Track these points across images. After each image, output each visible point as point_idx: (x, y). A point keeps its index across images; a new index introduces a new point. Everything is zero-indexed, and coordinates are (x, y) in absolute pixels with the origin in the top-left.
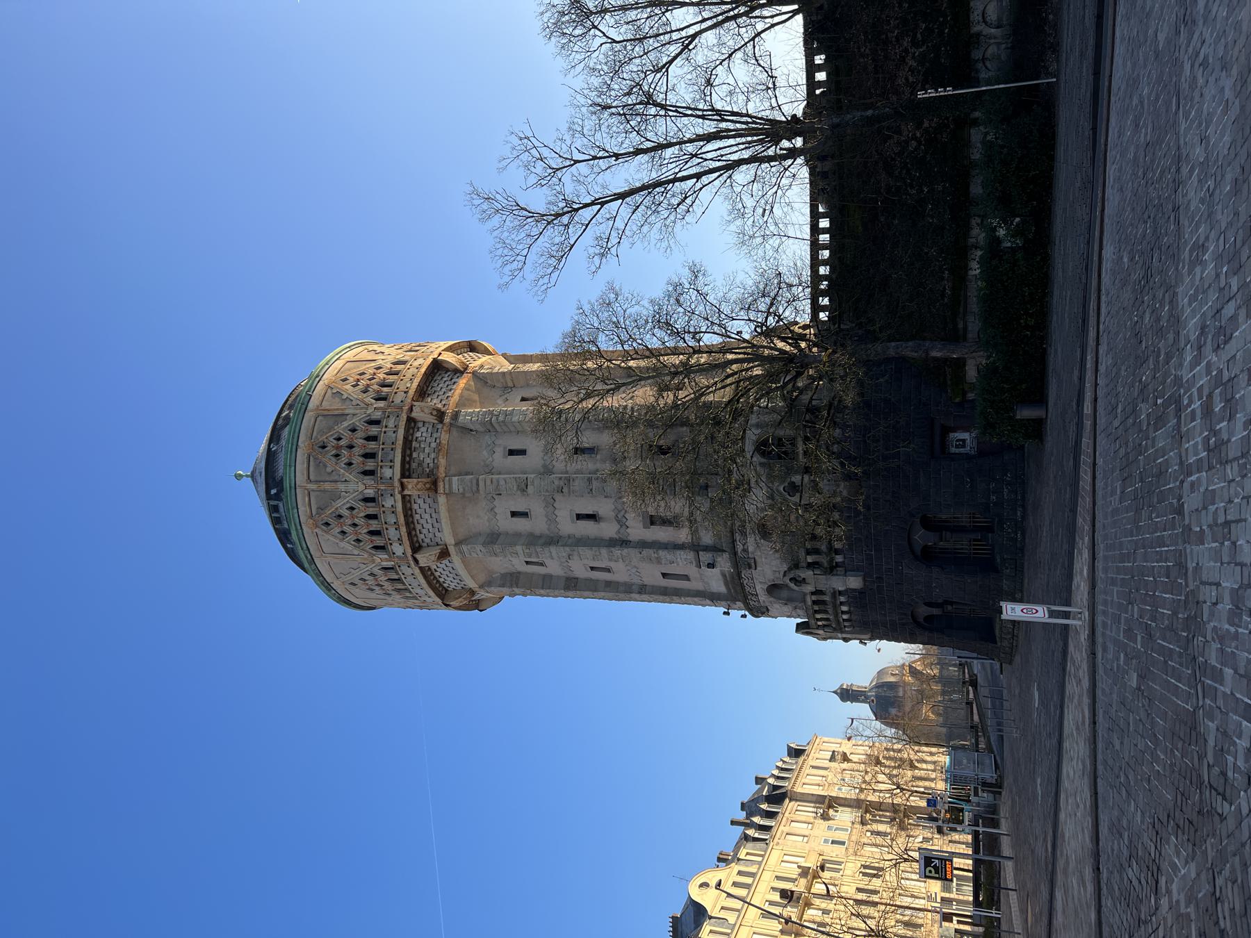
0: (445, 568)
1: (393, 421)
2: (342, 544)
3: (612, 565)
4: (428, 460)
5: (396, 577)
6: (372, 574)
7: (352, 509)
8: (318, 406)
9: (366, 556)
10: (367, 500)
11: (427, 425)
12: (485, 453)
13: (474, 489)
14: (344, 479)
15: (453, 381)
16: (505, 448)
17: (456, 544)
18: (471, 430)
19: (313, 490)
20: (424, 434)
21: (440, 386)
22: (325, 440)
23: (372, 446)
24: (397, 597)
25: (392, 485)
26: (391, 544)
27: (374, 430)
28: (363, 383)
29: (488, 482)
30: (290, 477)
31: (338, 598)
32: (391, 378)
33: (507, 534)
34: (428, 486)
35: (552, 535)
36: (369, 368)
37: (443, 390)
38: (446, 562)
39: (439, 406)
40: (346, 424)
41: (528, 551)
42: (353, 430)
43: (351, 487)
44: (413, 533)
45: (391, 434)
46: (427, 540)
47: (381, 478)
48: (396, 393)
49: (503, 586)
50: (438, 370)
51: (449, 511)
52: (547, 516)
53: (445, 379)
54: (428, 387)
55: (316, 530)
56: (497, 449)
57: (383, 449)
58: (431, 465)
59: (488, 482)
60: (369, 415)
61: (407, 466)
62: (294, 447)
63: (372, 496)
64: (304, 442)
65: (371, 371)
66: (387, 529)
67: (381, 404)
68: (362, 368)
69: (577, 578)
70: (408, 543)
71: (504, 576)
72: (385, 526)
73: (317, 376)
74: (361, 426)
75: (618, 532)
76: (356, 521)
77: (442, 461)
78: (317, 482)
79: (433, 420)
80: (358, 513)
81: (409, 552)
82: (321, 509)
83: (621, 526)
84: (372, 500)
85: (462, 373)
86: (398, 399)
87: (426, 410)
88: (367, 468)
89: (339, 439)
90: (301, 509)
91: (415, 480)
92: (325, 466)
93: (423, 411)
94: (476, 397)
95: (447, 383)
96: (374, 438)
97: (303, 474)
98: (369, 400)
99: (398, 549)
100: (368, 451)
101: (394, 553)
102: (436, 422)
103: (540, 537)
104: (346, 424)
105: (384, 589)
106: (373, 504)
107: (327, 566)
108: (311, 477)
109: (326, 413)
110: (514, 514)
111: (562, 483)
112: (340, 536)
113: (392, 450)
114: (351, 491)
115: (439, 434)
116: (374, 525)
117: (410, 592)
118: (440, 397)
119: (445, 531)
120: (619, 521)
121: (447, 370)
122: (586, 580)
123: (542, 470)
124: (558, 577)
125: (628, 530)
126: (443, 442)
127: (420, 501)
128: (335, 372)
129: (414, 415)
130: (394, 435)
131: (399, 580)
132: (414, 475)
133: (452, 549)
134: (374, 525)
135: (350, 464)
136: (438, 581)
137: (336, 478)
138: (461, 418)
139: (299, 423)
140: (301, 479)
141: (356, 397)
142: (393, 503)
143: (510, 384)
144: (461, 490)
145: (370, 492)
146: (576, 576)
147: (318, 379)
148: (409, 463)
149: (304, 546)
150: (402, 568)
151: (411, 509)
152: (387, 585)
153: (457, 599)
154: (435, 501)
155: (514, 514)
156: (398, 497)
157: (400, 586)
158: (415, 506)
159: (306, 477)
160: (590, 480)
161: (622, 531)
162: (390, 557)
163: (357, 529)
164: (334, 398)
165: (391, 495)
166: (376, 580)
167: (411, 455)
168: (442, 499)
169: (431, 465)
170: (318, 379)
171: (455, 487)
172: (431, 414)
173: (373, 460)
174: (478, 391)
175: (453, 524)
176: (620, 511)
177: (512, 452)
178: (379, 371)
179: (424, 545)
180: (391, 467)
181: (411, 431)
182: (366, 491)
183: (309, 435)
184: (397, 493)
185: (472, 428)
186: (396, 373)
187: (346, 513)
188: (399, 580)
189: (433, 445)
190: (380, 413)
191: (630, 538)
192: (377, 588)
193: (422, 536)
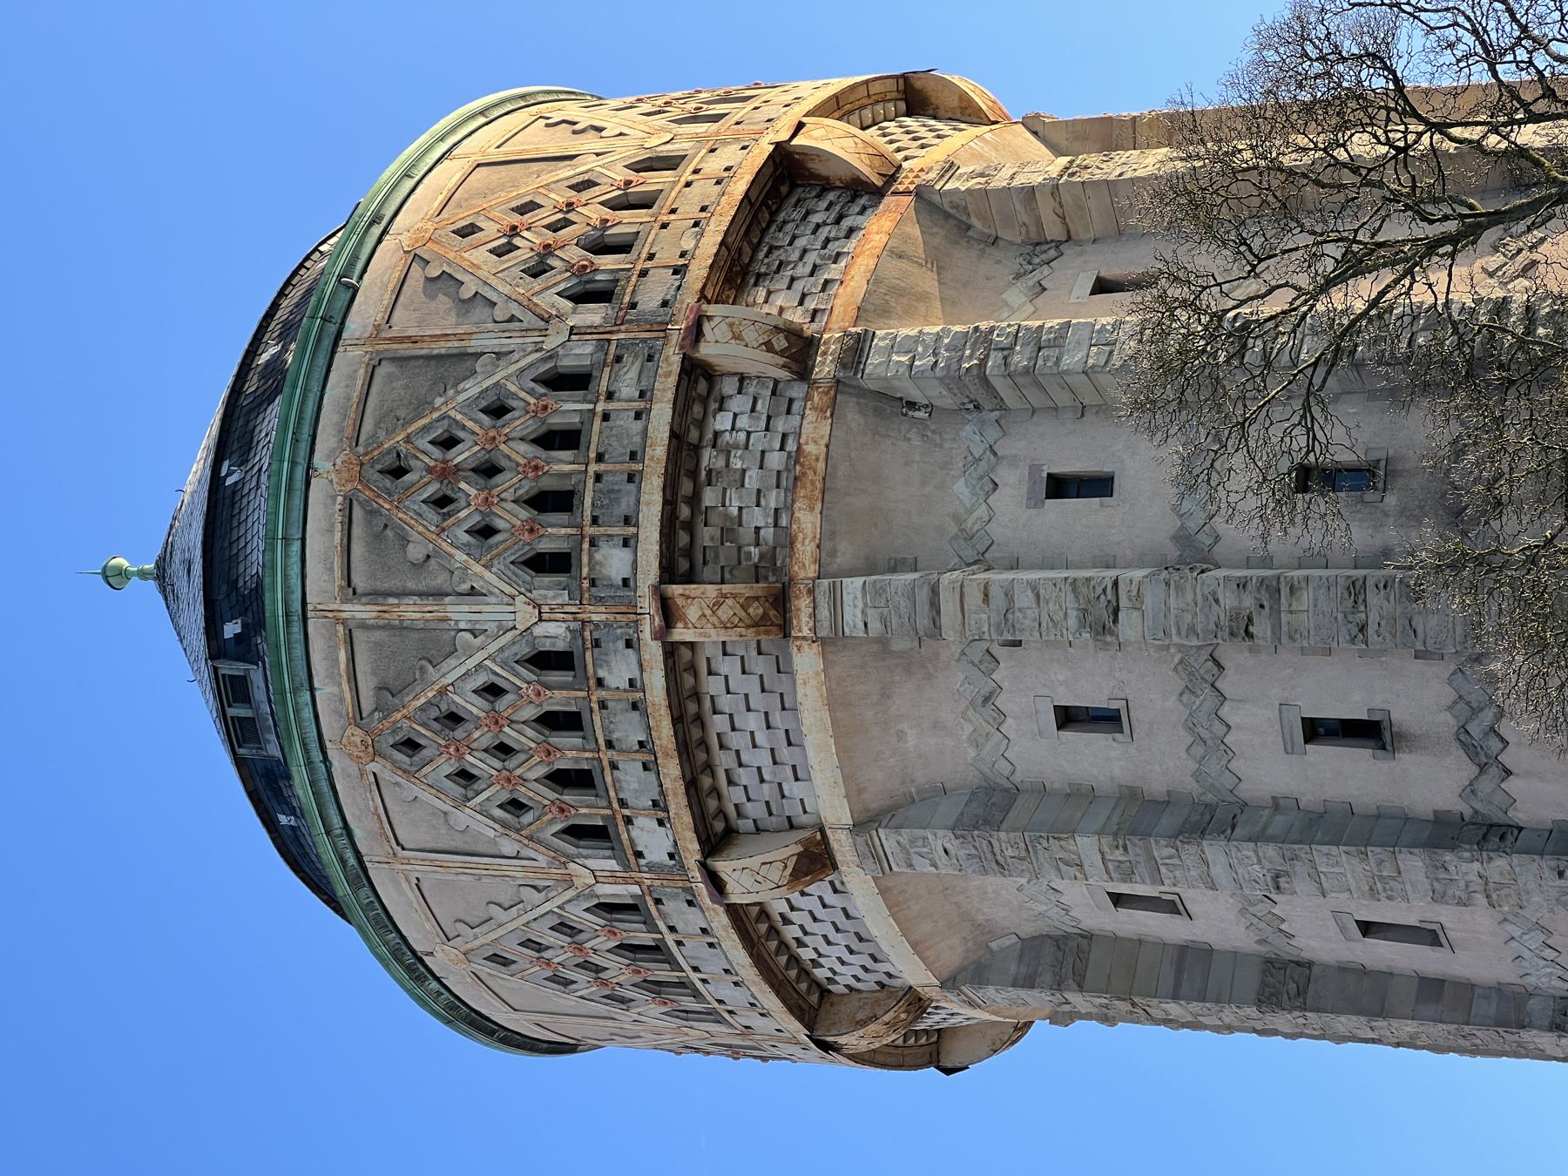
0: (820, 912)
1: (633, 374)
2: (463, 817)
3: (1444, 916)
4: (757, 518)
5: (646, 938)
6: (563, 927)
7: (493, 691)
8: (377, 327)
9: (542, 861)
10: (544, 660)
11: (751, 389)
12: (961, 488)
13: (923, 622)
14: (465, 587)
15: (846, 223)
16: (1034, 469)
17: (862, 825)
18: (912, 405)
19: (363, 626)
20: (743, 422)
21: (801, 243)
22: (403, 448)
23: (562, 463)
24: (651, 1011)
25: (632, 608)
27: (568, 409)
28: (530, 241)
29: (974, 597)
30: (286, 577)
31: (451, 1007)
32: (628, 222)
33: (1042, 791)
34: (756, 610)
35: (1209, 798)
36: (551, 187)
37: (811, 258)
38: (820, 888)
39: (797, 317)
40: (471, 388)
41: (1118, 855)
43: (491, 613)
45: (625, 422)
46: (755, 810)
47: (593, 583)
48: (644, 273)
49: (1029, 982)
50: (793, 187)
51: (835, 702)
52: (1191, 727)
53: (816, 218)
54: (755, 249)
55: (373, 767)
56: (1005, 475)
57: (598, 478)
58: (768, 534)
59: (974, 597)
60: (552, 355)
61: (683, 539)
62: (300, 472)
63: (561, 646)
64: (331, 455)
65: (561, 197)
66: (614, 766)
67: (593, 315)
68: (527, 184)
69: (1310, 965)
70: (687, 818)
71: (1032, 946)
72: (606, 754)
73: (374, 221)
74: (522, 393)
75: (1470, 790)
76: (510, 735)
77: (807, 521)
78: (376, 595)
79: (770, 367)
82: (389, 691)
83: (1483, 768)
85: (878, 193)
86: (650, 297)
87: (750, 335)
88: (545, 546)
89: (449, 443)
90: (325, 691)
91: (711, 591)
92: (404, 540)
93: (737, 337)
94: (927, 281)
95: (824, 232)
96: (566, 439)
98: (551, 301)
99: (652, 841)
100: (548, 484)
101: (639, 855)
102: (783, 374)
103: (1167, 803)
104: (471, 388)
105: (605, 983)
107: (413, 896)
108: (356, 579)
109: (404, 349)
110: (1067, 717)
111: (1248, 602)
112: (456, 790)
113: (631, 478)
114: (492, 627)
115: (795, 420)
116: (570, 751)
117: (697, 995)
118: (799, 286)
119: (817, 776)
120: (1471, 750)
121: (825, 185)
122: (1343, 969)
123: (1173, 553)
124: (1235, 954)
125: (1511, 785)
126: (809, 448)
127: (729, 666)
128: (437, 204)
129: (706, 351)
130: (639, 425)
131: (656, 951)
132: (707, 573)
133: (842, 844)
134: (570, 751)
135: (485, 532)
136: (794, 960)
137: (441, 580)
138: (874, 360)
139: (316, 388)
140: (321, 583)
141: (506, 290)
142: (636, 674)
143: (1053, 230)
144: (875, 627)
146: (1306, 955)
147: (376, 231)
148: (689, 527)
149: (336, 822)
150: (668, 906)
151: (696, 695)
152: (618, 970)
153: (863, 1024)
154: (782, 667)
155: (1067, 717)
156: (653, 651)
157: (662, 973)
158: (713, 686)
159: (339, 580)
160: (1356, 590)
161: (1486, 785)
162: (626, 867)
163: (511, 764)
164: (432, 297)
166: (579, 947)
167: (694, 500)
168: (806, 661)
169: (768, 534)
170: (376, 231)
171: (852, 617)
172: (769, 347)
173: (563, 517)
174: (937, 262)
175: (844, 753)
176: (1475, 711)
177: (1059, 487)
178: (585, 195)
179: (745, 825)
180: (626, 543)
181: (697, 410)
183: (349, 432)
184: (646, 634)
185: (915, 395)
186: (646, 202)
187: (474, 706)
188: (656, 951)
189: (776, 460)
190: (589, 349)
191: (1519, 816)
192: (581, 977)
193: (734, 795)
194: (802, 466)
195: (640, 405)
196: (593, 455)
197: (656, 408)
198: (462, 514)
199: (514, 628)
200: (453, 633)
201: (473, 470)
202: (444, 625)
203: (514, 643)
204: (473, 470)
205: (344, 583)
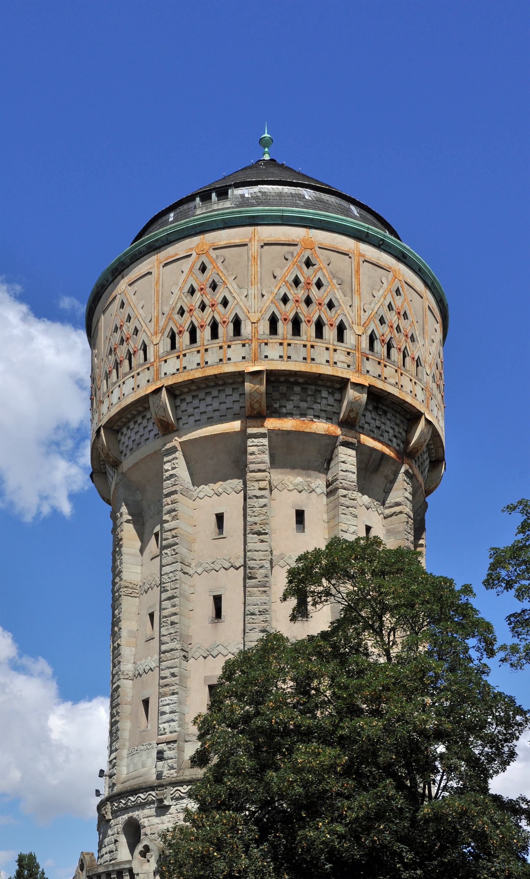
10: (237, 323)
26: (178, 357)
42: (331, 305)
44: (194, 388)
45: (326, 355)
76: (208, 310)
80: (219, 313)
81: (170, 382)
84: (237, 331)
89: (319, 285)
96: (319, 334)
97: (270, 236)
106: (231, 334)
145: (246, 329)
165: (244, 358)
182: (248, 323)
194: (308, 423)
196: (313, 344)
197: (330, 368)
198: (292, 291)
199: (249, 312)
200: (247, 287)
201: (308, 296)
202: (250, 284)
203: (243, 312)
204: (308, 296)
205: (266, 242)
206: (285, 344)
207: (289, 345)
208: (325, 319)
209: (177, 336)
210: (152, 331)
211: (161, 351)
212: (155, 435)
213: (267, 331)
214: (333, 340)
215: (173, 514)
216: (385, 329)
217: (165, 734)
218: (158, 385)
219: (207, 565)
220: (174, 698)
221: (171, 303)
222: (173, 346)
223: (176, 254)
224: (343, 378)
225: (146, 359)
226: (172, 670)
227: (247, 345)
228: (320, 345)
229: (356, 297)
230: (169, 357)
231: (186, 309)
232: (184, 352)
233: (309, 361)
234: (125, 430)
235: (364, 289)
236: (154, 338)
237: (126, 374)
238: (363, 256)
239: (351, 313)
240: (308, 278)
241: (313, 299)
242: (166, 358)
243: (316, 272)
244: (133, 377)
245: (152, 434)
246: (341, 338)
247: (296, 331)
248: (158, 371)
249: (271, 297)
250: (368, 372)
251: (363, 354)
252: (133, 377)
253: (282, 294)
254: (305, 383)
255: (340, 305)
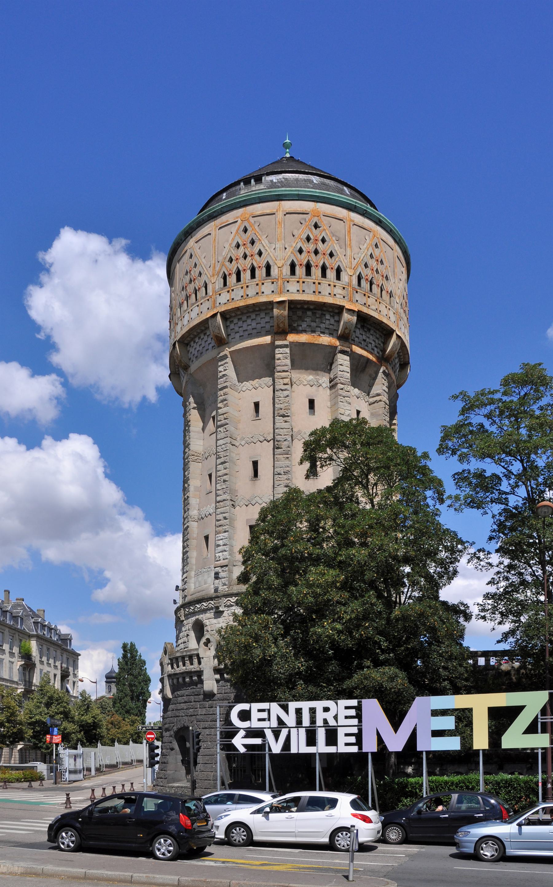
10: (268, 267)
26: (228, 292)
44: (239, 313)
45: (328, 290)
63: (272, 273)
76: (249, 259)
80: (256, 261)
84: (268, 273)
89: (323, 241)
96: (324, 275)
106: (265, 275)
130: (327, 294)
145: (274, 272)
165: (273, 292)
182: (276, 267)
195: (332, 295)
196: (320, 281)
197: (331, 299)
203: (272, 260)
205: (287, 212)
206: (301, 282)
207: (304, 282)
208: (327, 265)
209: (228, 277)
210: (211, 274)
211: (217, 287)
212: (213, 347)
213: (289, 273)
214: (333, 279)
215: (225, 402)
216: (368, 271)
217: (220, 560)
218: (215, 311)
219: (248, 439)
220: (226, 534)
221: (223, 254)
222: (225, 284)
223: (227, 221)
224: (340, 306)
225: (206, 294)
226: (224, 515)
227: (275, 283)
228: (324, 282)
229: (348, 250)
230: (222, 291)
231: (234, 258)
232: (232, 288)
233: (317, 293)
234: (192, 343)
235: (354, 243)
236: (212, 278)
237: (193, 304)
238: (353, 221)
239: (345, 260)
240: (316, 236)
241: (320, 251)
242: (220, 292)
243: (321, 232)
244: (198, 306)
245: (211, 346)
246: (338, 277)
247: (308, 273)
248: (215, 302)
249: (291, 250)
250: (357, 301)
251: (354, 289)
252: (198, 306)
253: (299, 247)
254: (315, 309)
255: (338, 255)
